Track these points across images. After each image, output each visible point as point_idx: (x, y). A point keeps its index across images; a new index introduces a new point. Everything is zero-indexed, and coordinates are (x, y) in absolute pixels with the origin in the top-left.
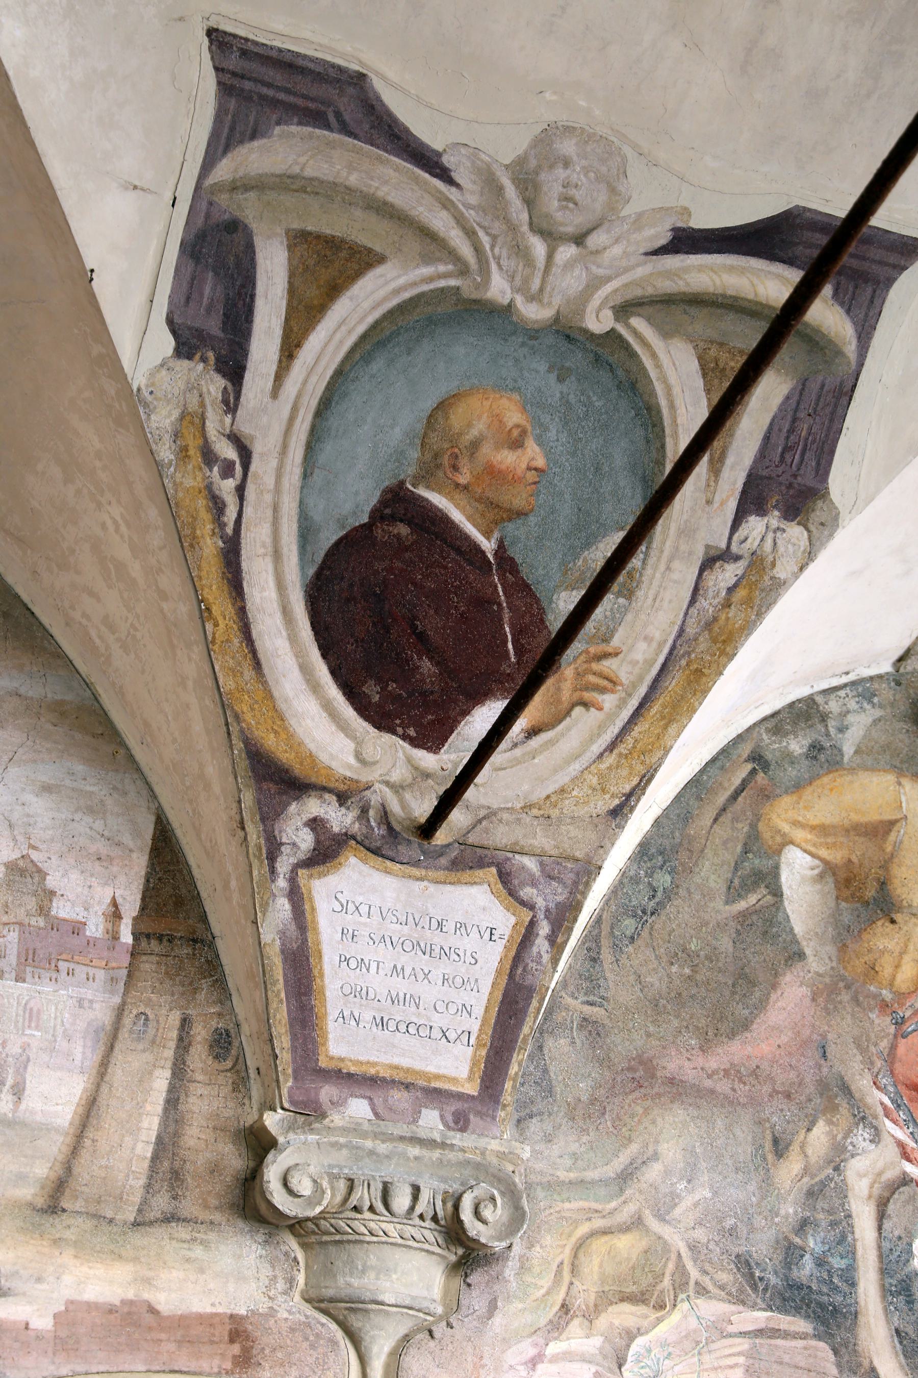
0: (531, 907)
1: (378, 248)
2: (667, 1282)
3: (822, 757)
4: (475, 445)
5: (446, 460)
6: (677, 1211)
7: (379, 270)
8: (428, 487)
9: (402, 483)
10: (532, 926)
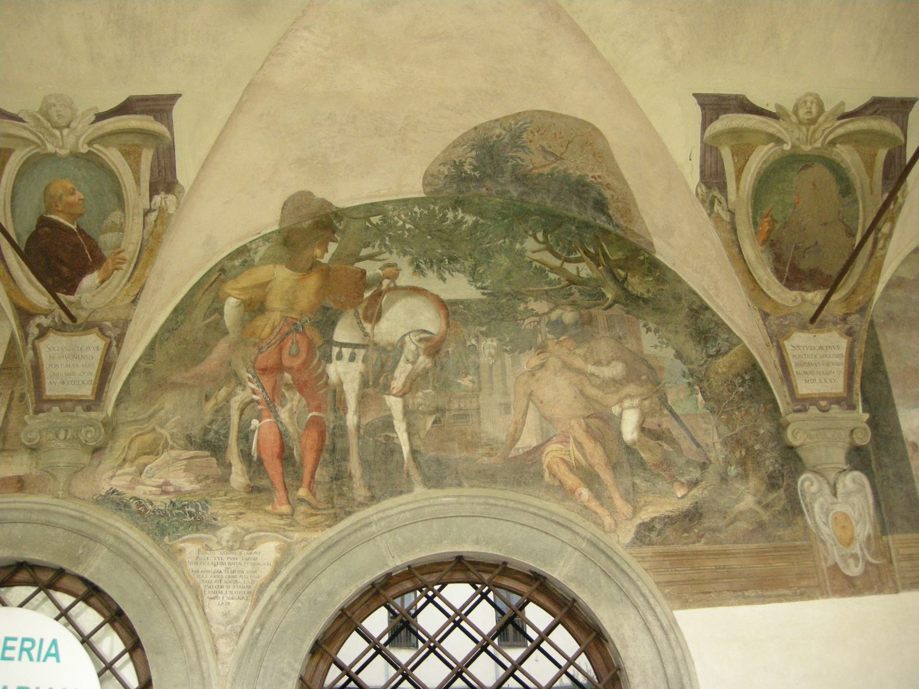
0: (109, 337)
1: (11, 147)
2: (160, 447)
3: (247, 264)
4: (61, 197)
5: (53, 204)
6: (167, 425)
7: (14, 154)
8: (51, 214)
9: (42, 216)
10: (110, 343)
